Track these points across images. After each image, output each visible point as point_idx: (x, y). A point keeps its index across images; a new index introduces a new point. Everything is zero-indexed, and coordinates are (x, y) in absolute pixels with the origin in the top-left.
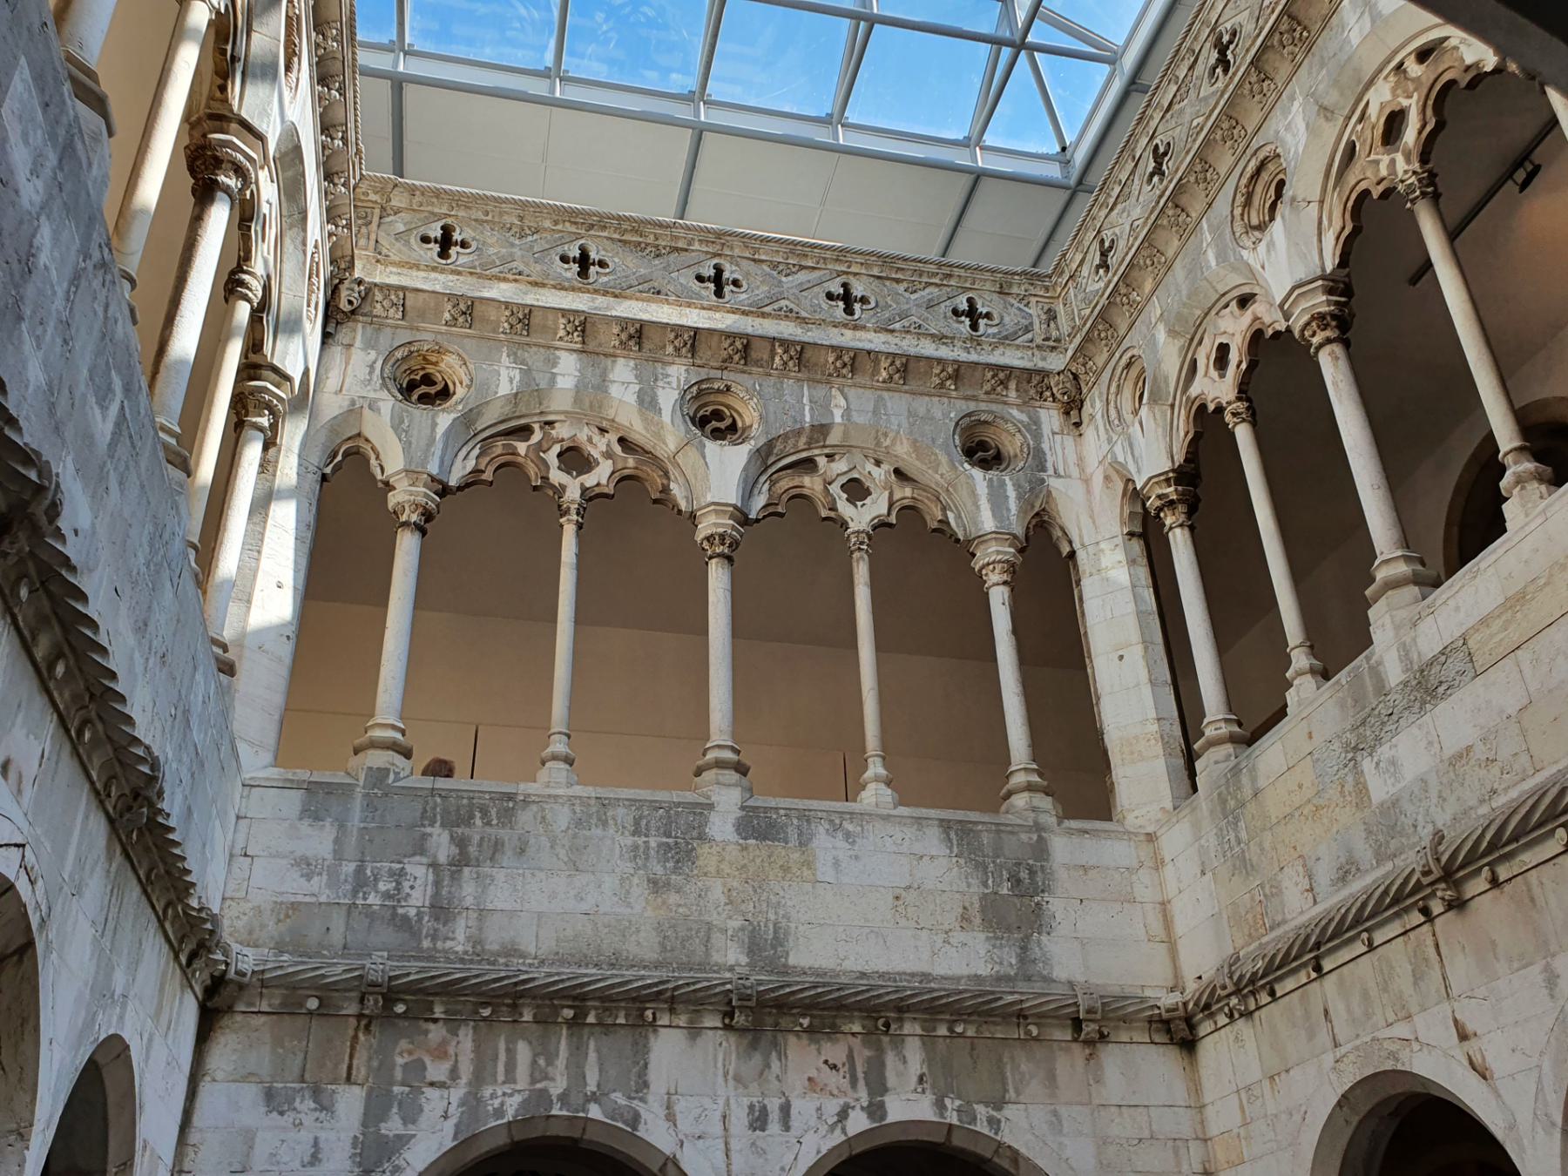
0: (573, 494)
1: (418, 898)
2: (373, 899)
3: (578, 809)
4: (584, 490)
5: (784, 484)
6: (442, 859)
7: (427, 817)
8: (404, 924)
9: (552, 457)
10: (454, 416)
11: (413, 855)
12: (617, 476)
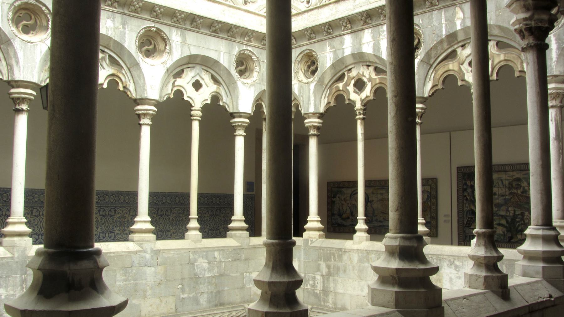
0: (358, 106)
1: (319, 287)
2: (309, 287)
3: (360, 254)
4: (362, 101)
5: (440, 72)
6: (324, 273)
7: (319, 258)
8: (316, 296)
9: (351, 88)
10: (315, 83)
11: (317, 271)
12: (374, 89)
